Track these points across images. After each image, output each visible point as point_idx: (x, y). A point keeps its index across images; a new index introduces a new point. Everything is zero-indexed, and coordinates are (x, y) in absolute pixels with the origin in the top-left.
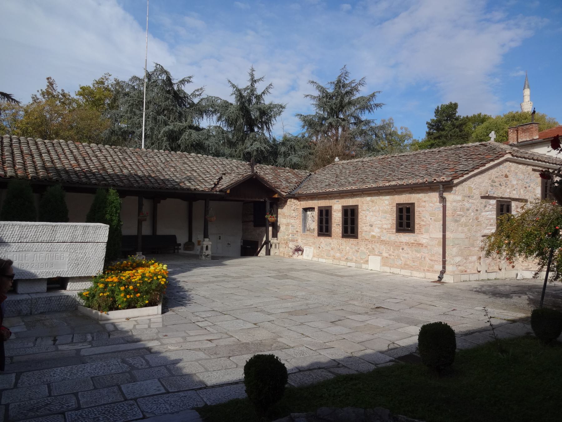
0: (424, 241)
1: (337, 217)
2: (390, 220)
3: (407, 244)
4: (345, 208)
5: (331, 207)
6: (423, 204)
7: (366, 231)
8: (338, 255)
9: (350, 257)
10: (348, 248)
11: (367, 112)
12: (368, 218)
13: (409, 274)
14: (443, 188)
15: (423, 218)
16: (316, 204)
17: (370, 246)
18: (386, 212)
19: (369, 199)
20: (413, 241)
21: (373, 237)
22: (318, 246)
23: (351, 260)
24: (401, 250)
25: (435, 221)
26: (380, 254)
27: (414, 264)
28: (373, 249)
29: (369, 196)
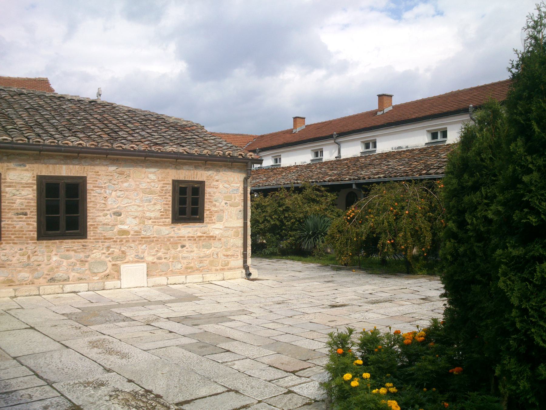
0: (217, 233)
2: (161, 204)
3: (190, 238)
6: (215, 183)
8: (25, 275)
10: (55, 258)
12: (110, 201)
13: (201, 280)
15: (214, 203)
18: (151, 192)
20: (199, 234)
23: (67, 280)
24: (179, 249)
25: (231, 206)
26: (140, 259)
27: (201, 265)
28: (123, 252)
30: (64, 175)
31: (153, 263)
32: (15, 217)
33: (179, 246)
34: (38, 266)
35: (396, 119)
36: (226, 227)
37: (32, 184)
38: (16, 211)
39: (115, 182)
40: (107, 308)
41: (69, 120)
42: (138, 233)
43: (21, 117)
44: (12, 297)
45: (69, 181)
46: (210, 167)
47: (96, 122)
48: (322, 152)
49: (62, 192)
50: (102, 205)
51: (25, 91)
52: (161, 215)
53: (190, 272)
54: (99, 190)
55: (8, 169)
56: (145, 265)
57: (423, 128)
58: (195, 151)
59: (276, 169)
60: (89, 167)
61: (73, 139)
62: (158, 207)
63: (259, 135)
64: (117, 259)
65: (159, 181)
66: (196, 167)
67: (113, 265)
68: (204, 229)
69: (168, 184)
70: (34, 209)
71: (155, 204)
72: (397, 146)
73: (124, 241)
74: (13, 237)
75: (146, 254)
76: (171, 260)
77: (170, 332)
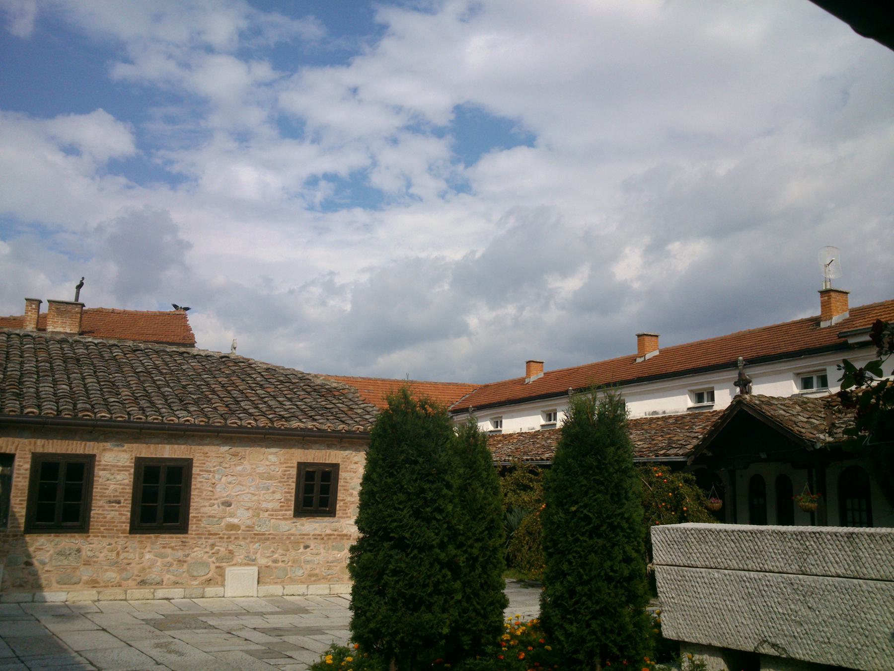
3: (317, 537)
5: (94, 456)
6: (353, 466)
8: (112, 575)
10: (148, 556)
13: (327, 592)
18: (270, 478)
20: (329, 532)
21: (233, 527)
23: (160, 583)
24: (302, 550)
26: (250, 561)
27: (330, 572)
28: (231, 552)
32: (107, 506)
33: (302, 547)
34: (129, 564)
35: (653, 371)
37: (129, 467)
38: (108, 499)
40: (195, 617)
41: (184, 387)
42: (250, 528)
43: (128, 386)
44: (94, 601)
45: (172, 464)
47: (218, 388)
48: (555, 414)
49: (163, 476)
50: (210, 493)
51: (142, 346)
53: (315, 581)
54: (206, 475)
55: (104, 450)
56: (256, 569)
57: (684, 386)
58: (327, 426)
59: (493, 437)
60: (197, 447)
61: (181, 414)
62: (278, 496)
63: (483, 384)
64: (222, 560)
65: (281, 463)
66: (329, 446)
67: (217, 567)
68: (336, 525)
70: (129, 497)
71: (274, 492)
72: (651, 410)
73: (233, 537)
74: (102, 528)
75: (258, 555)
76: (290, 564)
77: (246, 640)
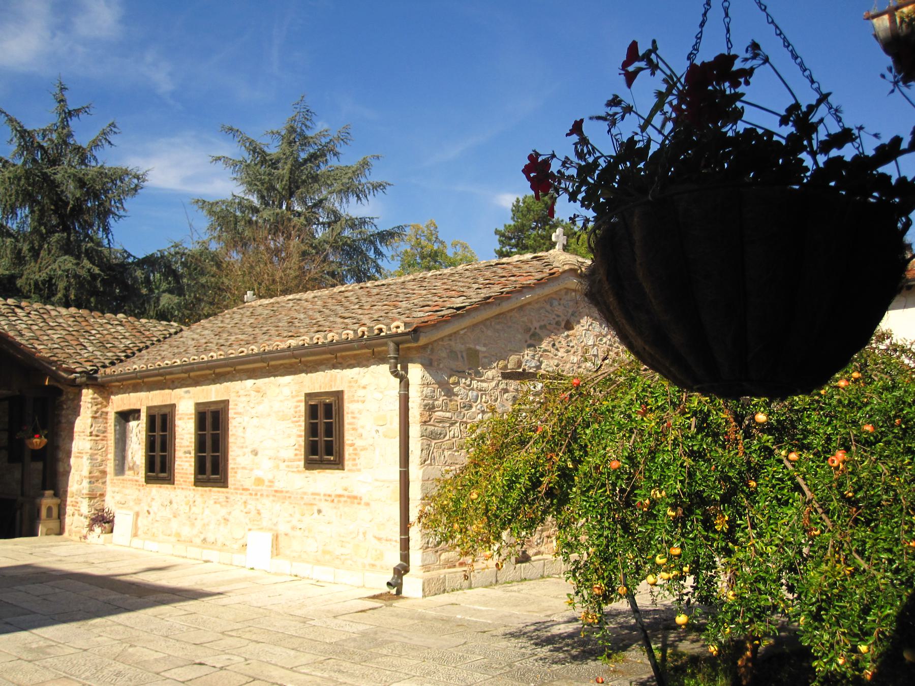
1: (185, 432)
2: (292, 435)
4: (202, 409)
5: (173, 406)
6: (361, 392)
7: (244, 468)
9: (211, 538)
11: (353, 199)
14: (397, 350)
16: (143, 400)
17: (252, 505)
19: (249, 383)
21: (259, 481)
22: (146, 508)
25: (385, 436)
28: (259, 513)
29: (250, 378)
30: (213, 399)
31: (286, 535)
32: (183, 455)
36: (377, 480)
39: (252, 405)
46: (353, 362)
52: (296, 455)
65: (293, 397)
69: (301, 401)
71: (289, 436)
